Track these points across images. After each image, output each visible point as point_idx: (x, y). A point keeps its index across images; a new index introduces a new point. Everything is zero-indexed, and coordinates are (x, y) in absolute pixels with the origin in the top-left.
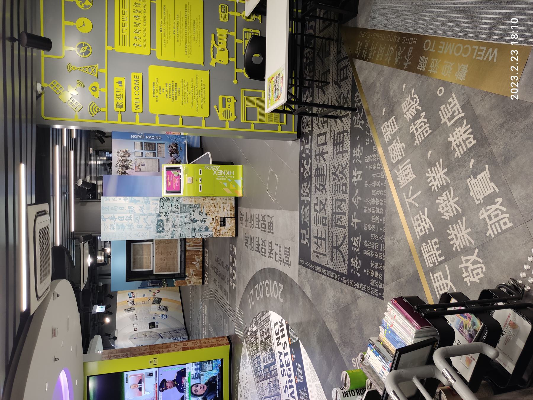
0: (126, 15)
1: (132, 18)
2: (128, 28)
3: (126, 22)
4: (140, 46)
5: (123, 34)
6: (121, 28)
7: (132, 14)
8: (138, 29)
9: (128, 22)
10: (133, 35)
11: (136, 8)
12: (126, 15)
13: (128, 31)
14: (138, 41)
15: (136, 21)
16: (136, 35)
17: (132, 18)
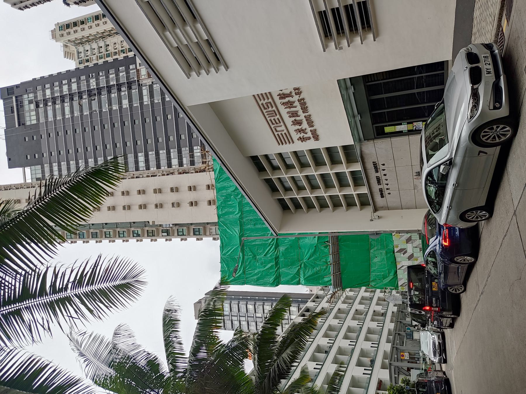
0: (270, 109)
1: (282, 108)
2: (282, 124)
3: (276, 118)
4: (309, 138)
5: (279, 133)
6: (272, 126)
8: (297, 118)
9: (278, 116)
10: (292, 129)
12: (270, 109)
13: (283, 128)
14: (303, 134)
15: (288, 110)
16: (298, 127)
17: (282, 108)
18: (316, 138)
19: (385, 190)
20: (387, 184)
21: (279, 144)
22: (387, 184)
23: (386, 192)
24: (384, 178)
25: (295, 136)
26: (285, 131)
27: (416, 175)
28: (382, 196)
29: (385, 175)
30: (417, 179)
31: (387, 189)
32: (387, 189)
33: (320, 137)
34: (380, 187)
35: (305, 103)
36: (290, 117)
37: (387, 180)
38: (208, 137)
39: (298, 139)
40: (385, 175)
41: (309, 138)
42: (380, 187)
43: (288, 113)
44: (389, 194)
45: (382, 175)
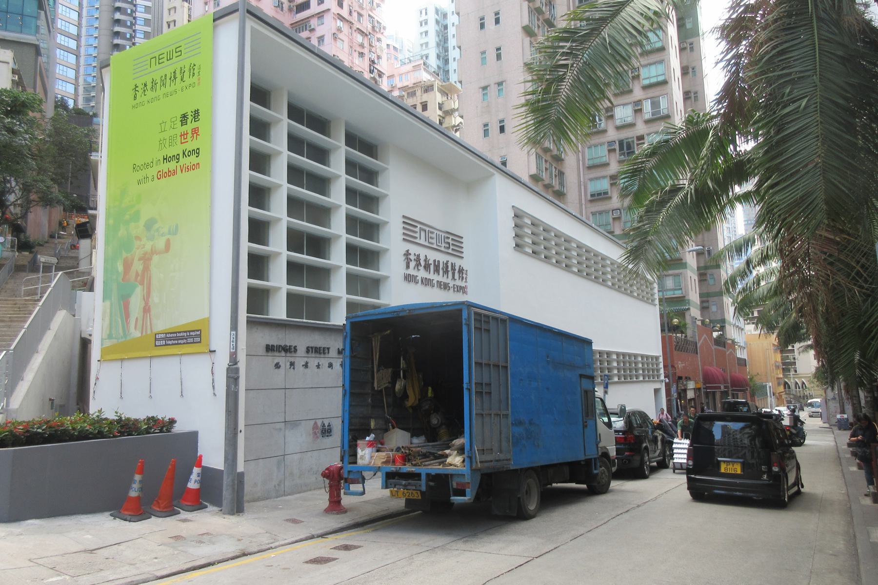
0: (443, 245)
4: (408, 267)
7: (452, 260)
11: (457, 268)
13: (422, 242)
18: (409, 278)
19: (292, 360)
20: (306, 366)
21: (404, 217)
22: (306, 366)
23: (283, 359)
24: (324, 362)
25: (414, 250)
26: (417, 241)
27: (324, 425)
28: (269, 349)
29: (330, 365)
30: (315, 426)
31: (292, 364)
32: (292, 364)
33: (406, 284)
34: (301, 350)
35: (445, 288)
36: (435, 261)
37: (318, 366)
38: (460, 151)
39: (408, 251)
40: (330, 365)
41: (408, 267)
42: (301, 350)
43: (439, 262)
44: (277, 366)
45: (331, 360)
